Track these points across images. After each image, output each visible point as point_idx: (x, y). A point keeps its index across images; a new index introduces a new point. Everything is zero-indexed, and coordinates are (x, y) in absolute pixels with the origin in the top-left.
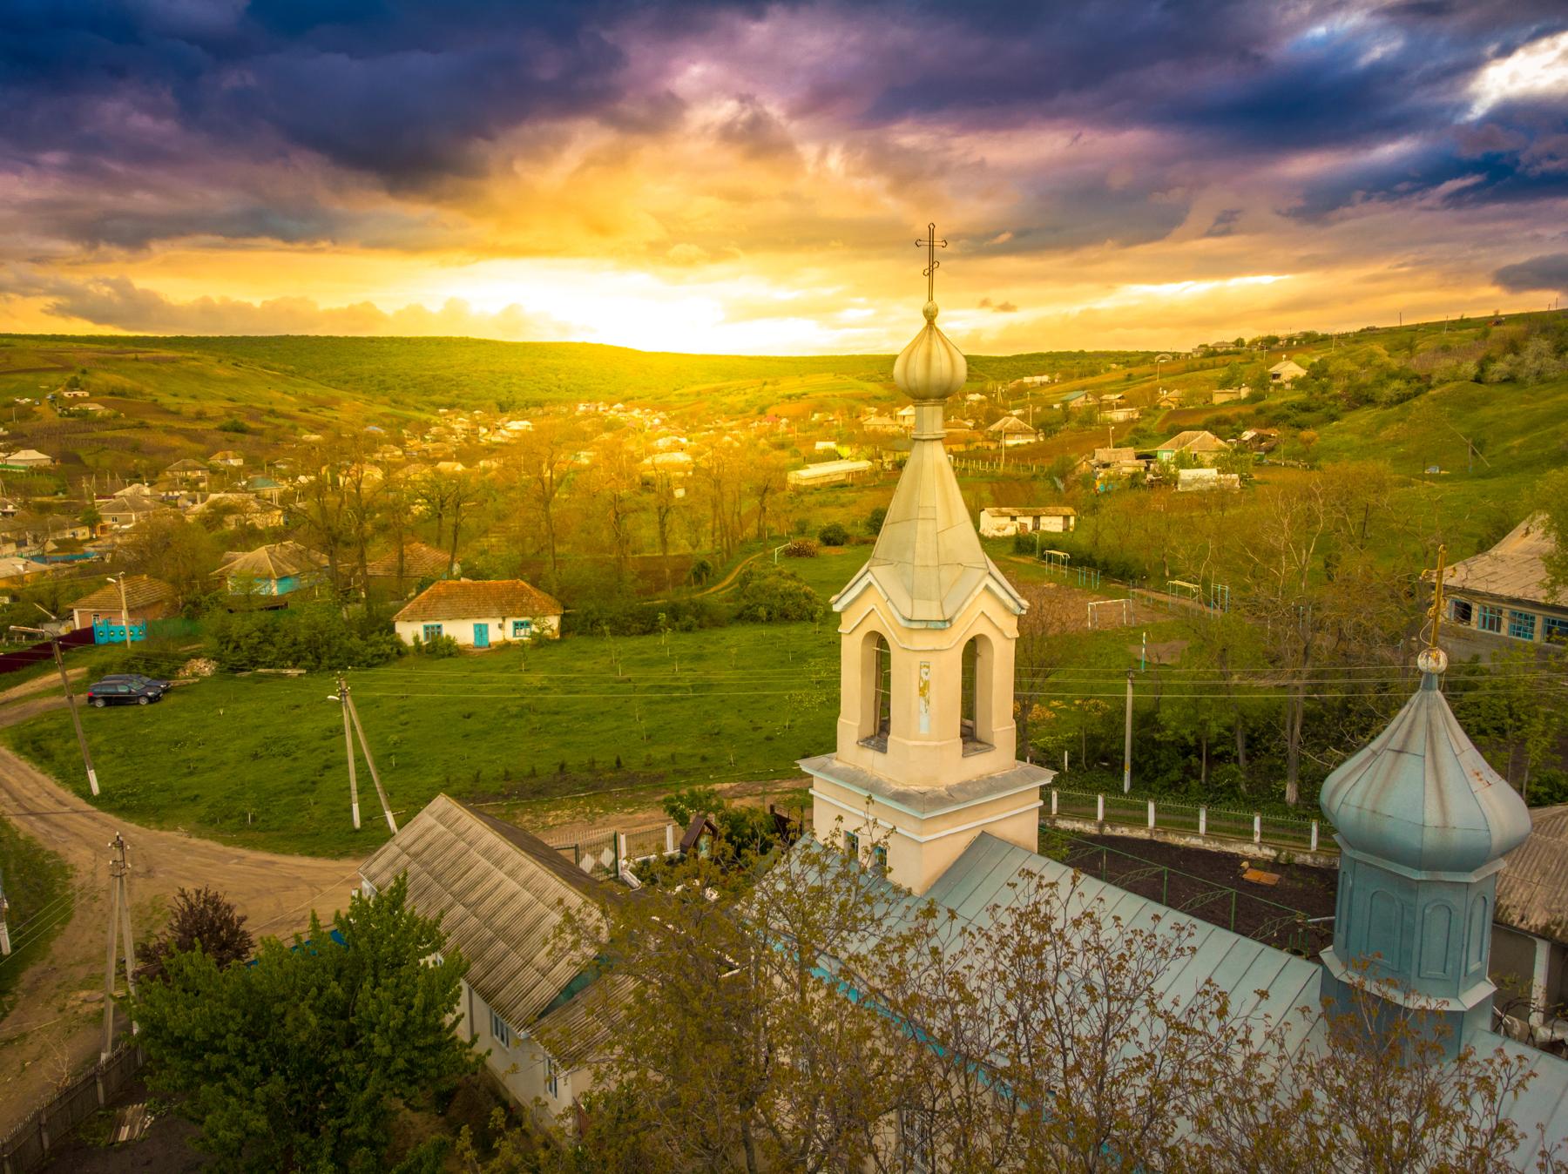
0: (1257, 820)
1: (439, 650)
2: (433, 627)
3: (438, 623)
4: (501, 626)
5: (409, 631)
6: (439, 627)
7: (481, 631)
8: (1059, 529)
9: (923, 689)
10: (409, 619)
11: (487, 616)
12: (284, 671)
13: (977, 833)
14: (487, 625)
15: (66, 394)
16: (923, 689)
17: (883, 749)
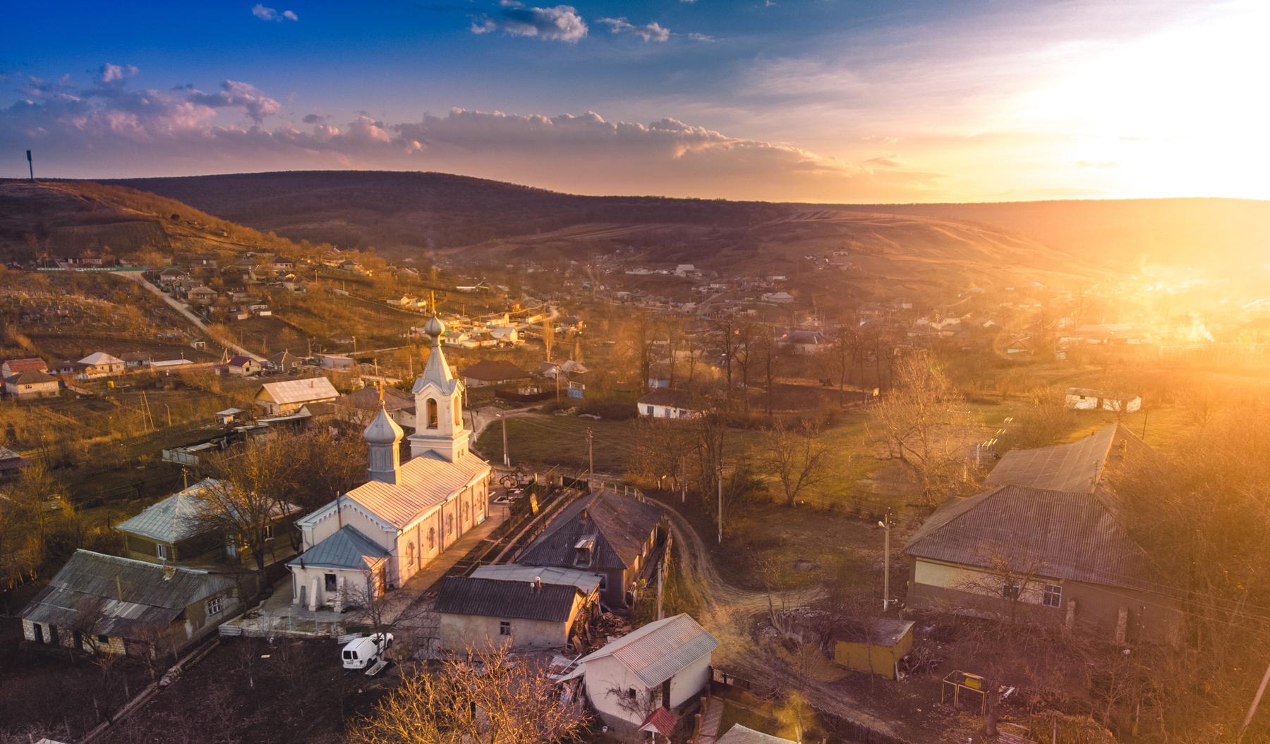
4: (675, 411)
5: (643, 408)
7: (668, 412)
11: (669, 405)
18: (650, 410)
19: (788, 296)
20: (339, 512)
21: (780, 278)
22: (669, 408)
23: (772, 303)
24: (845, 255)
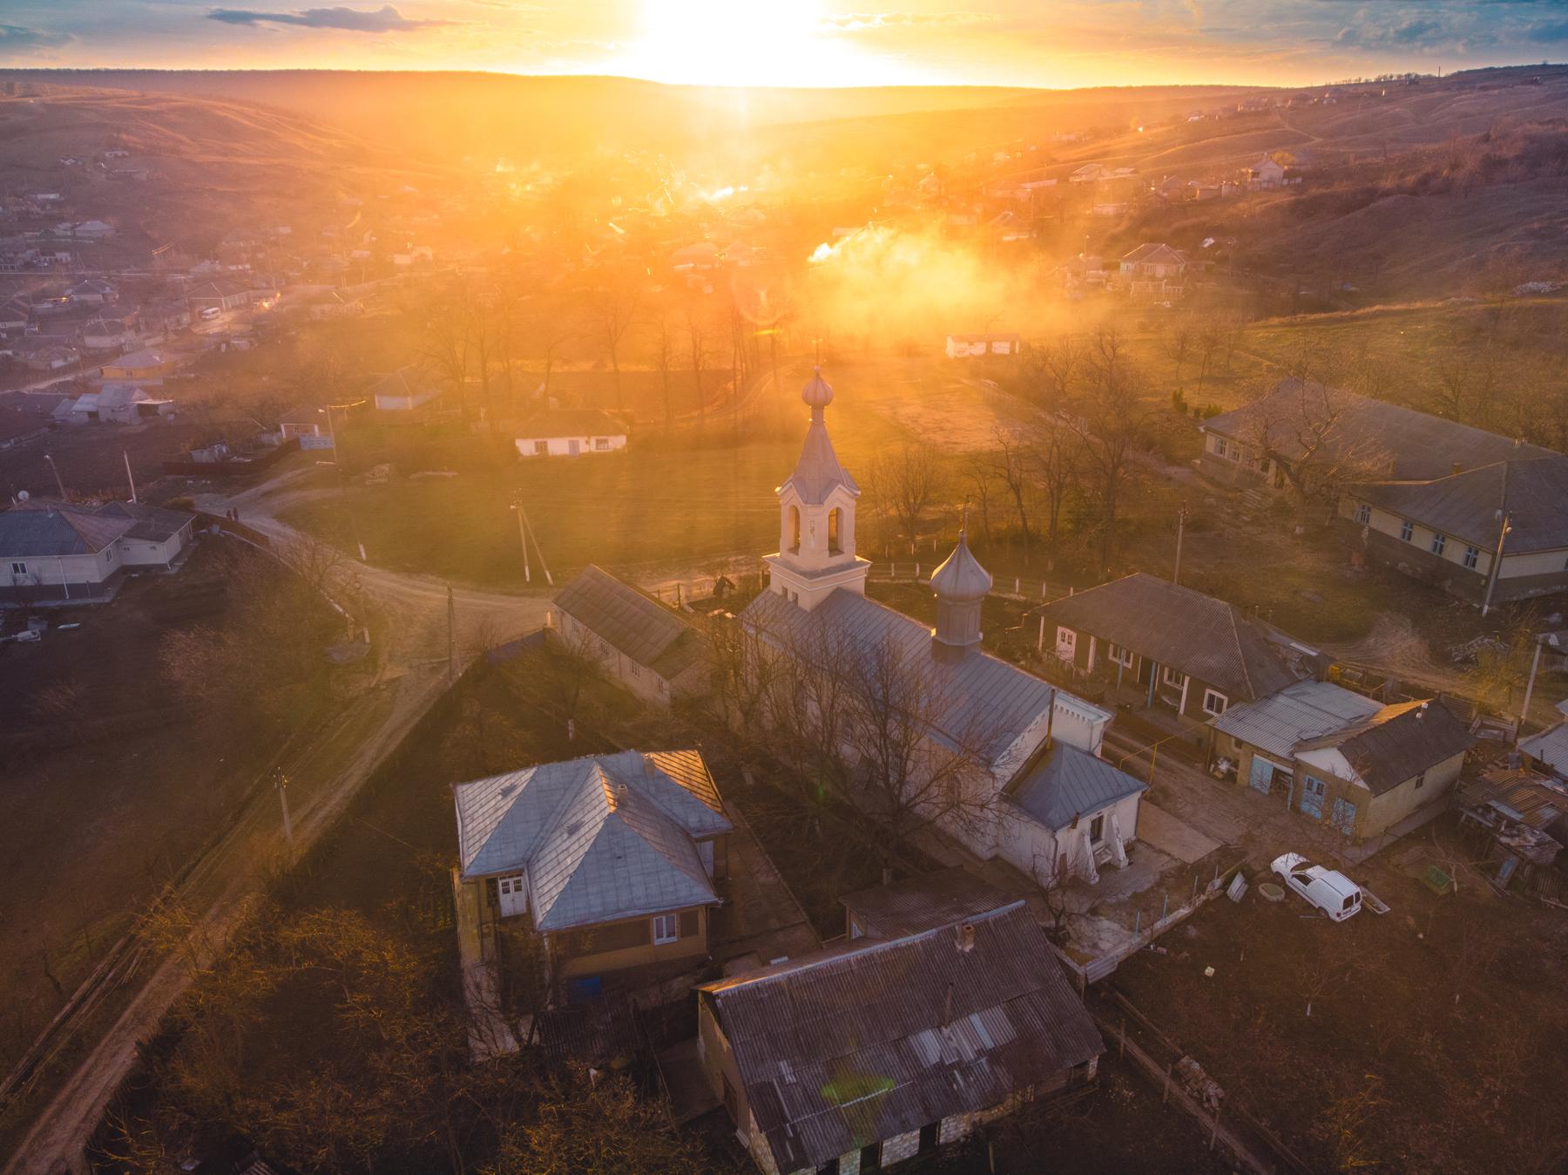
0: (1017, 581)
1: (542, 459)
2: (541, 443)
3: (545, 440)
4: (587, 442)
6: (545, 443)
7: (574, 446)
8: (1007, 351)
9: (812, 530)
10: (526, 436)
11: (577, 435)
12: (444, 474)
13: (835, 588)
14: (578, 441)
15: (107, 154)
16: (812, 530)
17: (797, 554)
18: (542, 447)
19: (105, 227)
20: (1050, 723)
21: (52, 196)
22: (575, 439)
23: (85, 238)
24: (124, 155)
